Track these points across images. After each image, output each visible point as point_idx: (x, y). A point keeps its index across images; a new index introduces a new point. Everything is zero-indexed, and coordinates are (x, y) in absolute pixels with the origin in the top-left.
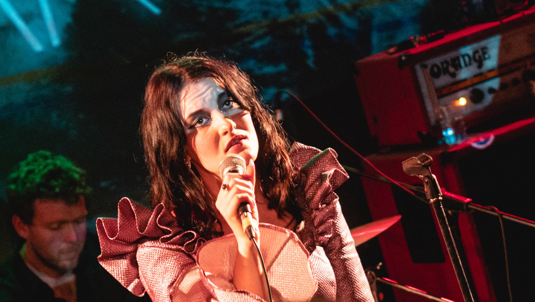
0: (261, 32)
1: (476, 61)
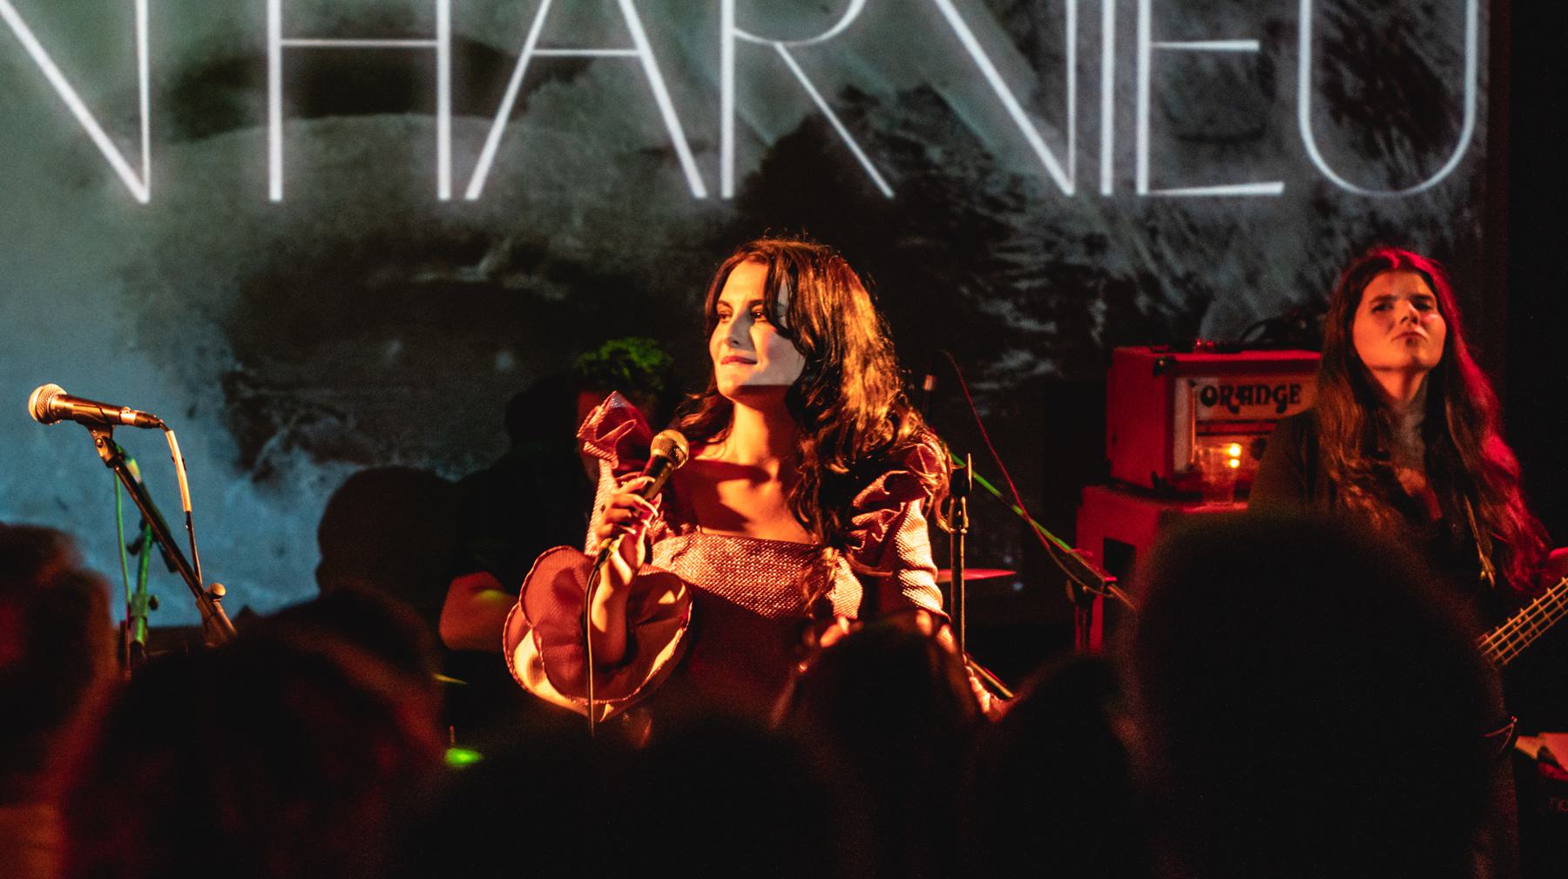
0: (1035, 268)
1: (1276, 400)
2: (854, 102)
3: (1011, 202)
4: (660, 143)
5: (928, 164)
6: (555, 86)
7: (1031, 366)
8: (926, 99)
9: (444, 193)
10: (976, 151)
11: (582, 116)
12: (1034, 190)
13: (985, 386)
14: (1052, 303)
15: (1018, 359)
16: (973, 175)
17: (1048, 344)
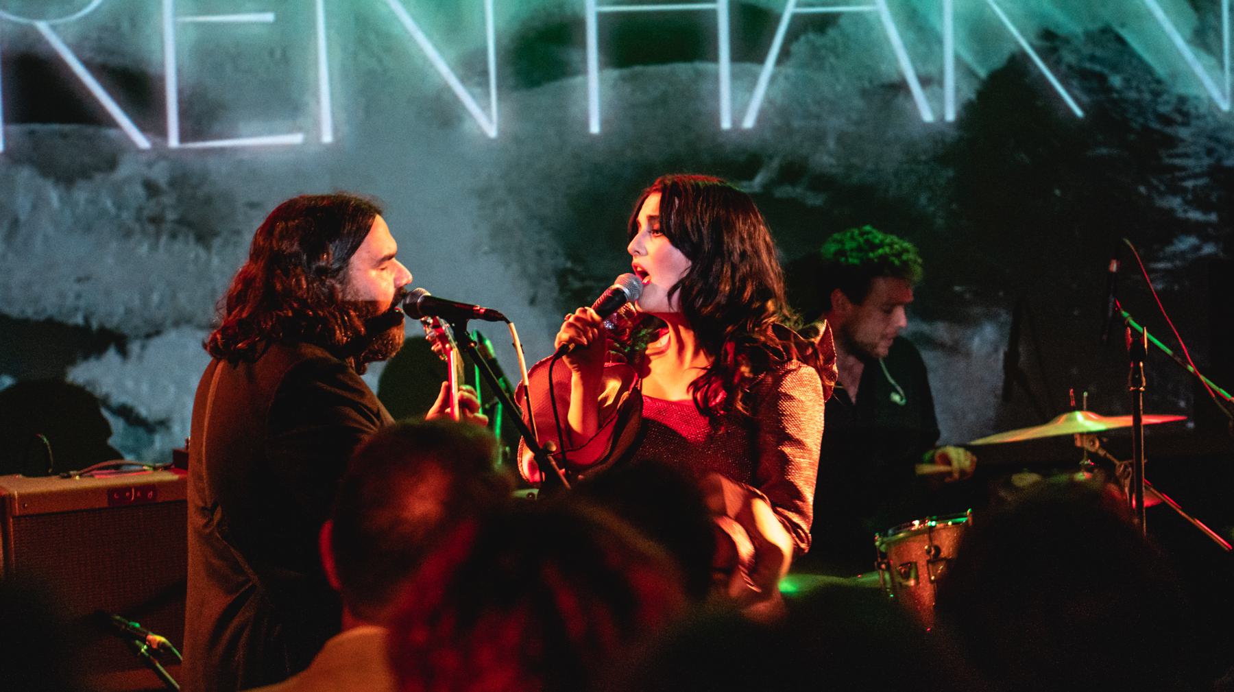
0: (1198, 170)
2: (1050, 41)
3: (1179, 118)
4: (895, 78)
5: (1111, 89)
6: (811, 36)
7: (1197, 249)
8: (1109, 37)
9: (726, 124)
10: (1149, 78)
11: (832, 60)
12: (1196, 108)
13: (1161, 265)
14: (1214, 198)
15: (1186, 243)
16: (1147, 96)
17: (1210, 230)
